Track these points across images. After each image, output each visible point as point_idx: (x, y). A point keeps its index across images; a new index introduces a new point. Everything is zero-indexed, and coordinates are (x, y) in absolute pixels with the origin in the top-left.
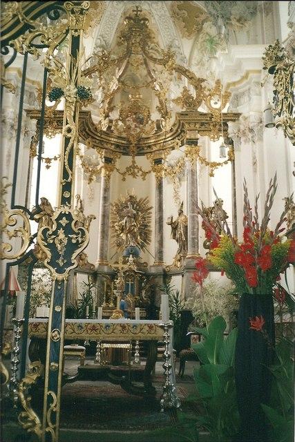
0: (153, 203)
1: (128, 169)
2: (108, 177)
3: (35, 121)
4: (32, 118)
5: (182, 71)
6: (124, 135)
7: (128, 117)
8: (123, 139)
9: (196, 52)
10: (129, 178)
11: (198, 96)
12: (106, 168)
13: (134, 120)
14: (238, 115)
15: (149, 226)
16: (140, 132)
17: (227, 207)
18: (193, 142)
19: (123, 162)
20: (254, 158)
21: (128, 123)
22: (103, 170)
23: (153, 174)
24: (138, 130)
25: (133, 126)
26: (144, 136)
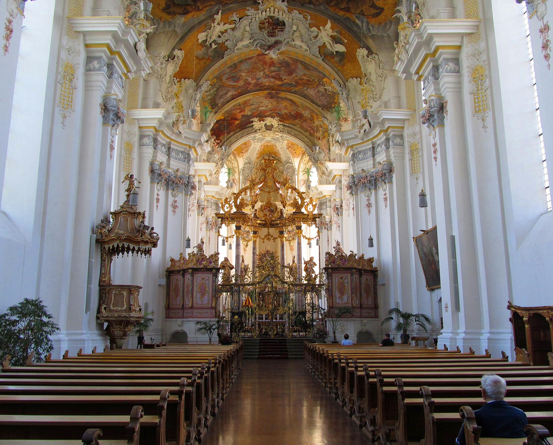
0: (279, 254)
2: (255, 242)
3: (220, 219)
4: (218, 218)
5: (294, 189)
6: (263, 219)
9: (302, 164)
11: (302, 202)
12: (254, 237)
14: (321, 215)
17: (316, 260)
18: (299, 228)
19: (264, 231)
20: (328, 238)
23: (279, 239)
26: (273, 219)
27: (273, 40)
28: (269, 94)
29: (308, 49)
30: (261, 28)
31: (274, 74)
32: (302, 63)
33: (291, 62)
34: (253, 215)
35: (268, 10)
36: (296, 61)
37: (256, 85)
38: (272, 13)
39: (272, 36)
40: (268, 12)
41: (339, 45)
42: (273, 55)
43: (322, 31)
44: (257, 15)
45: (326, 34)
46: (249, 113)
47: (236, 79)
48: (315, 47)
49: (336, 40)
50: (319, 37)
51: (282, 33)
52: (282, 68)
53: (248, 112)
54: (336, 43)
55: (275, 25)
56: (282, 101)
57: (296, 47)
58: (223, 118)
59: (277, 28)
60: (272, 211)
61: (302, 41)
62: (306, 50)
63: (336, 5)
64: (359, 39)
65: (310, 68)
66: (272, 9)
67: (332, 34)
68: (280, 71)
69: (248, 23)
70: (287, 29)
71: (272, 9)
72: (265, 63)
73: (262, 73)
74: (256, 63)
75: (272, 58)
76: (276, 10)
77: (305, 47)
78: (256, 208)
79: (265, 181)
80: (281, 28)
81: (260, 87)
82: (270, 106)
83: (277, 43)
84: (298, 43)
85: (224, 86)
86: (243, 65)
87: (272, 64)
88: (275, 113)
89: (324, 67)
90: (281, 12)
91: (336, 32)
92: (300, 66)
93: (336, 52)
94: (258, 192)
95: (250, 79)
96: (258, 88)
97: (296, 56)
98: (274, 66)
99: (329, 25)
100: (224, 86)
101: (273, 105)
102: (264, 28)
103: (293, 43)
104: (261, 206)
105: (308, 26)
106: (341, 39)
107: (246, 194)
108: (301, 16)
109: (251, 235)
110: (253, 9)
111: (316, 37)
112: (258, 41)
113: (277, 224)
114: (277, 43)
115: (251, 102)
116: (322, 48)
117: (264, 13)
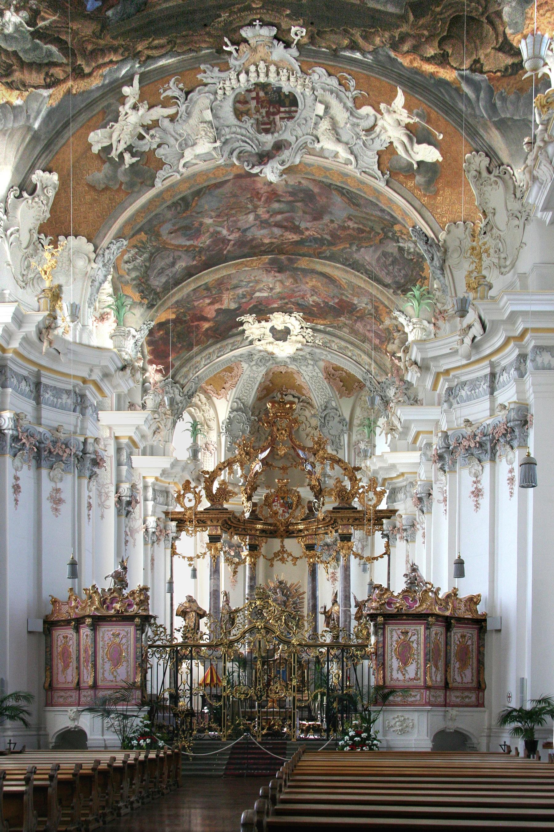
1: (276, 555)
2: (253, 566)
6: (270, 521)
7: (274, 501)
8: (270, 525)
10: (277, 564)
12: (250, 555)
13: (282, 506)
15: (302, 612)
16: (288, 518)
21: (275, 508)
22: (248, 558)
24: (287, 515)
25: (281, 512)
27: (268, 140)
28: (273, 262)
29: (352, 158)
30: (239, 114)
31: (279, 217)
32: (341, 191)
33: (316, 190)
34: (247, 515)
35: (252, 68)
36: (328, 187)
37: (241, 243)
38: (262, 75)
39: (267, 131)
40: (253, 75)
41: (425, 146)
42: (271, 173)
43: (386, 115)
44: (228, 83)
45: (393, 120)
46: (233, 306)
47: (190, 230)
48: (370, 153)
49: (417, 135)
50: (377, 129)
51: (290, 124)
52: (299, 204)
53: (228, 302)
54: (419, 142)
55: (272, 105)
56: (304, 277)
57: (326, 154)
58: (174, 316)
59: (279, 112)
60: (288, 506)
61: (339, 140)
62: (348, 162)
63: (415, 49)
64: (473, 133)
65: (362, 202)
66: (262, 65)
67: (408, 120)
68: (293, 210)
69: (208, 101)
70: (302, 112)
71: (262, 65)
72: (257, 195)
73: (251, 217)
74: (235, 196)
75: (271, 183)
76: (273, 68)
77: (343, 154)
78: (255, 499)
79: (273, 444)
80: (289, 112)
81: (249, 249)
82: (278, 289)
83: (279, 147)
84: (328, 144)
85: (167, 249)
86: (203, 201)
87: (273, 194)
88: (293, 303)
89: (390, 200)
90: (284, 73)
91: (418, 115)
92: (337, 199)
93: (420, 163)
94: (257, 467)
95: (225, 232)
96: (246, 250)
97: (326, 177)
98: (279, 201)
99: (400, 99)
100: (166, 249)
101: (284, 287)
102: (247, 113)
103: (318, 146)
104: (266, 497)
105: (350, 104)
106: (429, 133)
107: (232, 472)
108: (333, 82)
109: (245, 553)
110: (216, 69)
111: (370, 130)
112: (237, 144)
113: (301, 531)
114: (279, 147)
115: (234, 282)
116: (386, 156)
117: (243, 77)
